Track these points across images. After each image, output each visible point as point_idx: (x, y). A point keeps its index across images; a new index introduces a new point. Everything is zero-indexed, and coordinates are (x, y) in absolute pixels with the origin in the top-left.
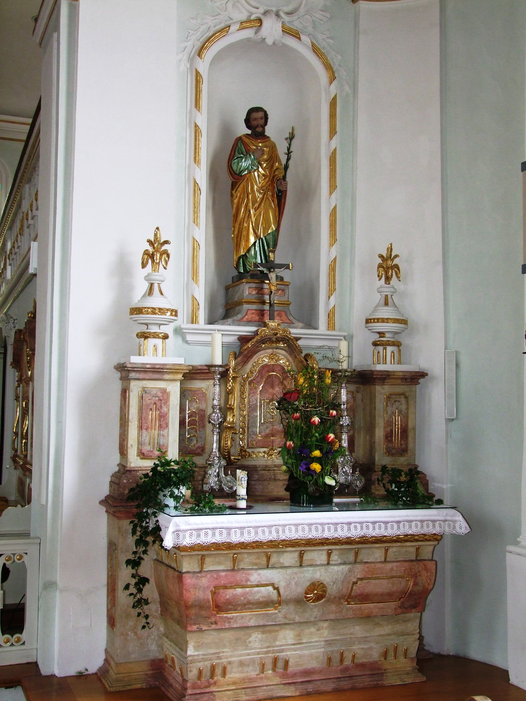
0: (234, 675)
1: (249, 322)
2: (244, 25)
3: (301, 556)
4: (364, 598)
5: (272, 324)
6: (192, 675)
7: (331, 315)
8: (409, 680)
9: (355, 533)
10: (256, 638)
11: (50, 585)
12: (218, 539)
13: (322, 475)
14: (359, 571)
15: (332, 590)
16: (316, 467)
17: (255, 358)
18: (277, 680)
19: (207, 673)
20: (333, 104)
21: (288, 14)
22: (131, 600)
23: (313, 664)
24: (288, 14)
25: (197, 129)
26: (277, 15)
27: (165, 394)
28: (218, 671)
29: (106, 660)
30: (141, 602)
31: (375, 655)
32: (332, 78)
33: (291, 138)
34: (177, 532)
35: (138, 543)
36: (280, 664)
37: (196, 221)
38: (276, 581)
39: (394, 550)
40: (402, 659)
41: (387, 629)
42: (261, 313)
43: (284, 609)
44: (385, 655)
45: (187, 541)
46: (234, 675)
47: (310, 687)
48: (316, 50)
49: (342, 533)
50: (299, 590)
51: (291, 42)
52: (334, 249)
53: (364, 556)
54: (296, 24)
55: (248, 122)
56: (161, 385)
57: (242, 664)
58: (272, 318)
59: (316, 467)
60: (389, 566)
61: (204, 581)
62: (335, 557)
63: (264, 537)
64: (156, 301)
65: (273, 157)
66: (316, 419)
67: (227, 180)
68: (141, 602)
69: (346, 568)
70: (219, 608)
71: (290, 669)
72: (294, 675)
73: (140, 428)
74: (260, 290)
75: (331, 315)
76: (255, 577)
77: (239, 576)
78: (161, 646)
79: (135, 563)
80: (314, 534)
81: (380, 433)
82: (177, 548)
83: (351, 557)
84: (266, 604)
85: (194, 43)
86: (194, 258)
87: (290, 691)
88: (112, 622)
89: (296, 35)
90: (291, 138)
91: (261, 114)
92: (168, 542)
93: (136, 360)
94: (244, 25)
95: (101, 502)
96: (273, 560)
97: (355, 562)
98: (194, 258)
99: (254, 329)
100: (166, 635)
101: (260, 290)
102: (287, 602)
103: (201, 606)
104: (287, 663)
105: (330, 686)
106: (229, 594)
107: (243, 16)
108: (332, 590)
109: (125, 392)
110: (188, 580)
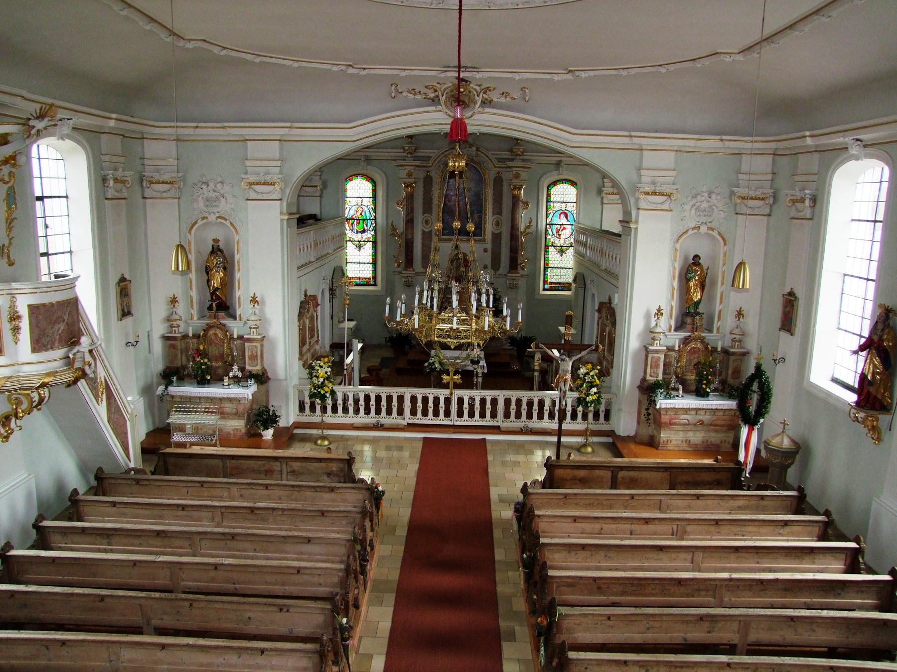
0: (674, 442)
1: (689, 331)
2: (693, 229)
3: (697, 412)
4: (716, 425)
5: (696, 333)
6: (662, 441)
7: (718, 329)
8: (730, 450)
9: (714, 407)
10: (681, 433)
11: (620, 410)
12: (672, 406)
13: (706, 388)
14: (715, 417)
15: (706, 422)
16: (704, 386)
17: (690, 345)
18: (686, 445)
19: (666, 441)
20: (725, 253)
21: (709, 222)
22: (645, 419)
23: (698, 442)
24: (709, 222)
25: (673, 288)
26: (706, 224)
27: (659, 358)
28: (669, 441)
29: (636, 433)
30: (648, 419)
31: (718, 442)
32: (725, 244)
33: (708, 269)
34: (660, 404)
35: (649, 404)
36: (688, 442)
37: (673, 298)
38: (688, 418)
39: (727, 412)
40: (726, 444)
41: (722, 435)
42: (693, 328)
43: (690, 426)
44: (721, 442)
45: (663, 406)
46: (674, 442)
47: (696, 449)
48: (719, 234)
49: (709, 407)
50: (695, 422)
51: (711, 232)
52: (721, 306)
53: (716, 413)
54: (713, 225)
55: (693, 259)
56: (658, 355)
57: (676, 440)
58: (696, 331)
59: (704, 386)
60: (724, 417)
61: (667, 417)
62: (707, 413)
63: (685, 407)
64: (658, 330)
65: (702, 271)
66: (705, 373)
67: (684, 280)
68: (648, 419)
69: (710, 416)
70: (671, 424)
71: (691, 443)
72: (692, 445)
73: (651, 368)
74: (693, 321)
75: (718, 329)
76: (682, 417)
77: (677, 416)
78: (653, 432)
79: (647, 409)
80: (701, 407)
81: (730, 372)
82: (660, 408)
83: (713, 413)
84: (685, 424)
85: (676, 237)
86: (671, 310)
87: (690, 449)
88: (638, 423)
89: (712, 229)
90: (708, 269)
91: (698, 258)
92: (658, 407)
93: (651, 348)
94: (693, 229)
95: (637, 387)
96: (688, 412)
97: (714, 415)
98: (671, 310)
99: (690, 334)
100: (655, 429)
101: (693, 321)
102: (691, 425)
103: (665, 423)
104: (690, 441)
105: (703, 449)
106: (674, 421)
107: (693, 225)
108: (706, 422)
109: (647, 356)
110: (663, 416)
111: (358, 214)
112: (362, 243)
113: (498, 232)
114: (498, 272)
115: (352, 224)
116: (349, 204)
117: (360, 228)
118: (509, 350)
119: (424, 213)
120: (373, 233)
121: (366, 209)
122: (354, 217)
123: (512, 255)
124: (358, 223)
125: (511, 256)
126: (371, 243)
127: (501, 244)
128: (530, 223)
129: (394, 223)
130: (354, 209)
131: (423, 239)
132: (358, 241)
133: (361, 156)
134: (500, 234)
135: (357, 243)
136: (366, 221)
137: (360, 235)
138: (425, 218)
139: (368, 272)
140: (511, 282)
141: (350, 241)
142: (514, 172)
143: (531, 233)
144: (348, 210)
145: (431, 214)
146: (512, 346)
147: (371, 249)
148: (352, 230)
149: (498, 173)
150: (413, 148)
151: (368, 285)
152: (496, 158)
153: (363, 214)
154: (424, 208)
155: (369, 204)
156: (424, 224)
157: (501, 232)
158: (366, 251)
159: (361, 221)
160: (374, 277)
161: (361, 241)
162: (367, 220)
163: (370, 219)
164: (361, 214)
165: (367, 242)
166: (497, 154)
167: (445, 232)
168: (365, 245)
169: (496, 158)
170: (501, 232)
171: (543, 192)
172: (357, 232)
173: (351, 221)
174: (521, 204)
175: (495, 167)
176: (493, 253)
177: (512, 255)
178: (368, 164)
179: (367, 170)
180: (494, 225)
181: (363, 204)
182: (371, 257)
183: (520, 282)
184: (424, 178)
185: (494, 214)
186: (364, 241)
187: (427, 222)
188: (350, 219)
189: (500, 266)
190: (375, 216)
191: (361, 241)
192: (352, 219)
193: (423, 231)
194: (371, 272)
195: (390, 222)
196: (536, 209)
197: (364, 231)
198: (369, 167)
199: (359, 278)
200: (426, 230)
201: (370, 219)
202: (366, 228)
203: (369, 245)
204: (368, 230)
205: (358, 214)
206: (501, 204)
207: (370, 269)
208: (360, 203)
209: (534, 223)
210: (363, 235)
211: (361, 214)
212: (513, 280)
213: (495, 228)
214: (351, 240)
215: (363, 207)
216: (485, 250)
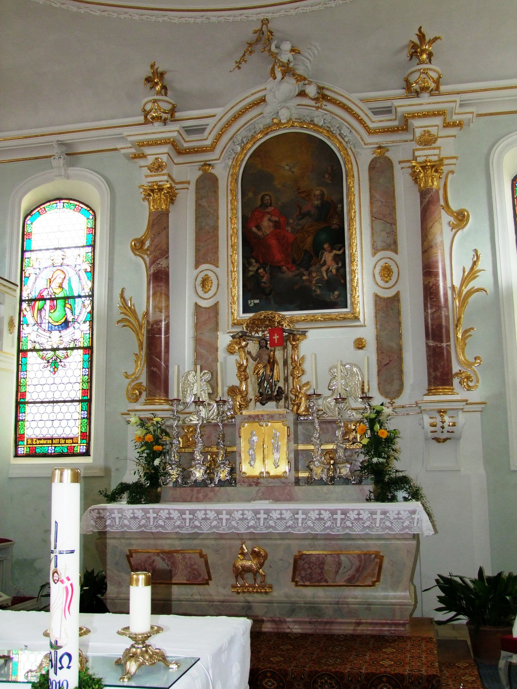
111: (55, 285)
112: (60, 353)
113: (389, 294)
114: (398, 402)
115: (40, 310)
116: (36, 265)
117: (58, 316)
118: (440, 623)
119: (197, 265)
120: (86, 327)
121: (71, 273)
122: (45, 294)
123: (431, 343)
124: (53, 308)
125: (428, 346)
126: (81, 351)
127: (400, 323)
128: (475, 263)
129: (127, 296)
130: (47, 274)
131: (198, 326)
132: (54, 350)
133: (49, 146)
134: (396, 298)
135: (50, 354)
136: (71, 301)
137: (56, 334)
138: (202, 275)
139: (72, 423)
140: (438, 420)
141: (34, 350)
142: (418, 132)
143: (478, 290)
144: (32, 277)
145: (215, 262)
146: (449, 608)
147: (80, 366)
148: (39, 324)
149: (380, 147)
150: (168, 107)
151: (71, 454)
152: (370, 109)
153: (65, 285)
154: (197, 250)
155: (80, 261)
156: (199, 289)
157: (398, 294)
158: (69, 373)
159: (60, 303)
160: (86, 436)
161: (58, 349)
162: (74, 297)
163: (80, 297)
164: (61, 286)
165: (72, 349)
166: (376, 100)
167: (252, 303)
168: (67, 357)
169: (370, 109)
170: (398, 294)
171: (501, 191)
172: (50, 330)
173: (39, 304)
174: (445, 218)
175: (370, 132)
176: (380, 350)
177: (431, 343)
178: (72, 165)
179: (68, 177)
180: (378, 278)
181: (65, 262)
182: (78, 387)
183: (461, 418)
184: (197, 181)
185: (375, 250)
186: (66, 349)
187: (205, 282)
188: (35, 300)
189: (402, 386)
190: (92, 290)
191: (58, 349)
192: (41, 298)
193: (196, 304)
194: (78, 422)
195: (117, 292)
196: (487, 225)
197: (66, 324)
198: (72, 171)
199: (52, 439)
200: (205, 304)
201: (80, 297)
202: (70, 318)
203: (78, 355)
204: (74, 321)
205: (55, 285)
206: (393, 223)
207: (77, 416)
208: (58, 262)
209: (485, 263)
210: (64, 333)
211: (61, 286)
212: (441, 412)
213: (381, 283)
214: (38, 347)
215: (64, 268)
216: (360, 344)
